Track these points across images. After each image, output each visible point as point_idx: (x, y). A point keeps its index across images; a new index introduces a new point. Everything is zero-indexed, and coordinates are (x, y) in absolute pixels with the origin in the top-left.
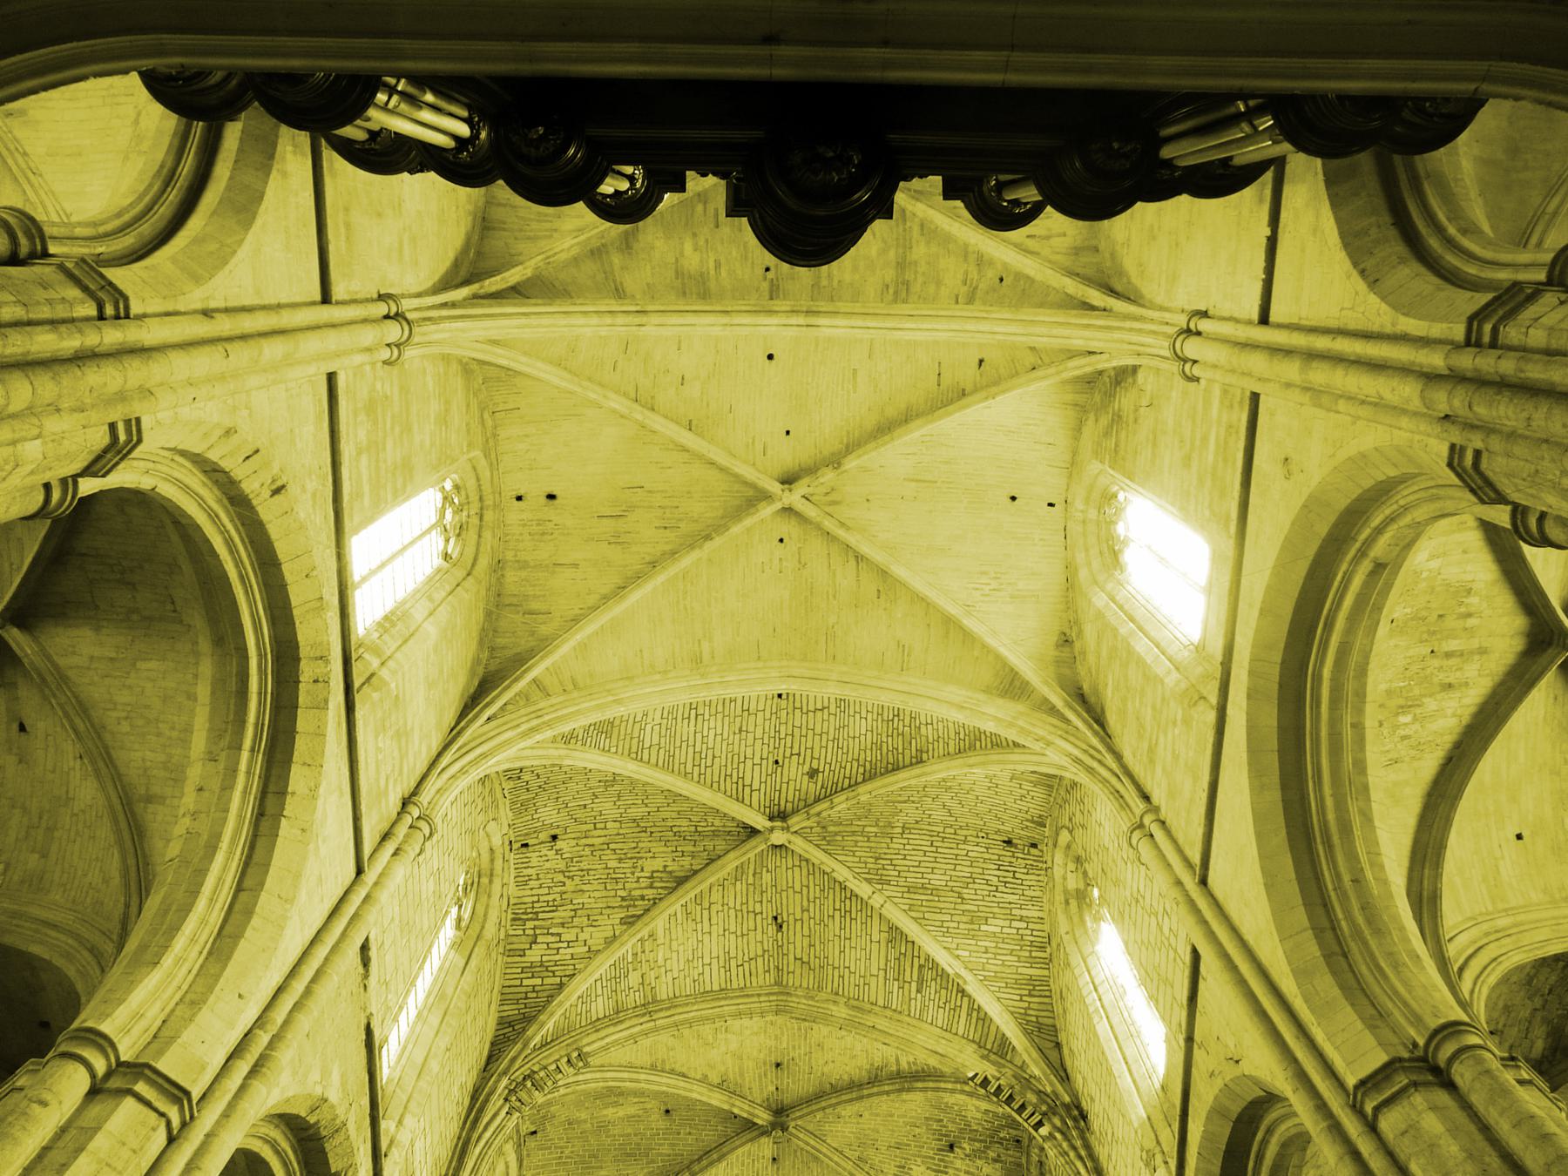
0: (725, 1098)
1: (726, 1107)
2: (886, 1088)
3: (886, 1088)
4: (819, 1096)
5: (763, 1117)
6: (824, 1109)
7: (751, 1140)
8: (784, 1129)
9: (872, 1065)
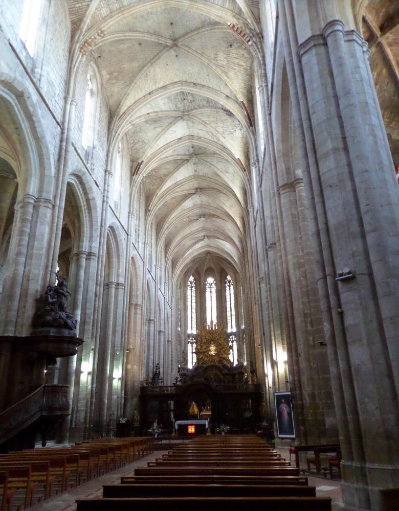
0: (156, 38)
1: (157, 41)
2: (207, 29)
3: (207, 29)
4: (187, 34)
5: (170, 43)
6: (188, 38)
7: (168, 51)
8: (177, 46)
9: (202, 21)
